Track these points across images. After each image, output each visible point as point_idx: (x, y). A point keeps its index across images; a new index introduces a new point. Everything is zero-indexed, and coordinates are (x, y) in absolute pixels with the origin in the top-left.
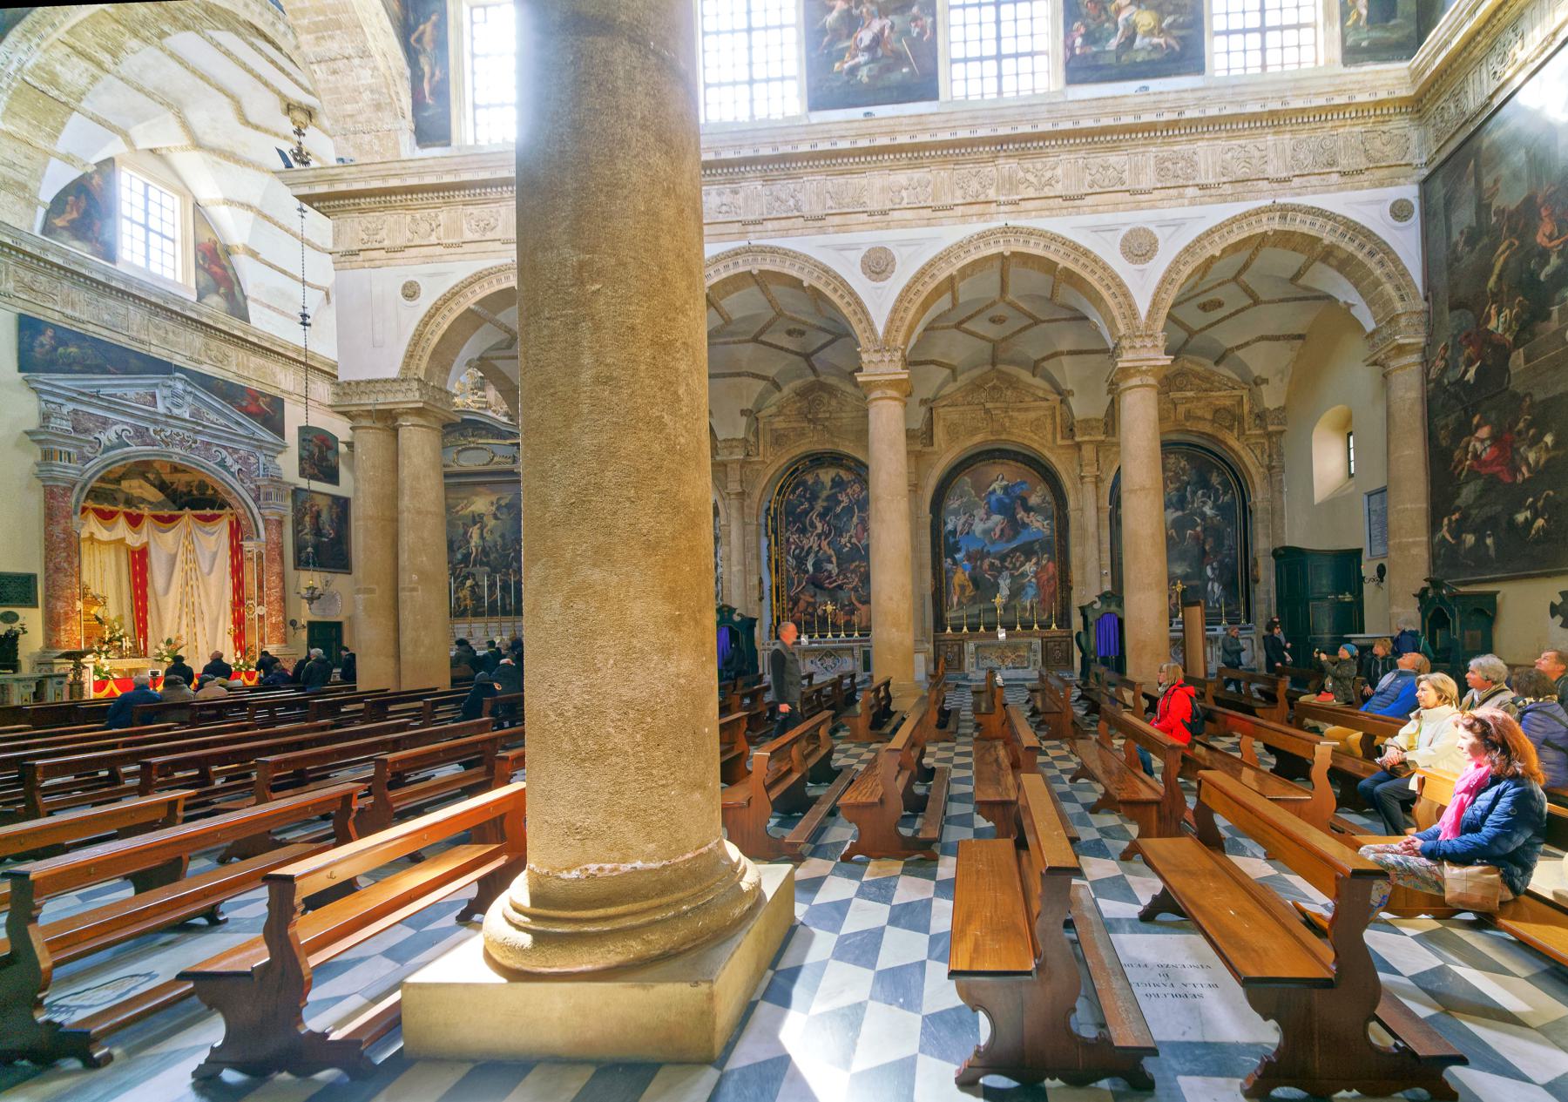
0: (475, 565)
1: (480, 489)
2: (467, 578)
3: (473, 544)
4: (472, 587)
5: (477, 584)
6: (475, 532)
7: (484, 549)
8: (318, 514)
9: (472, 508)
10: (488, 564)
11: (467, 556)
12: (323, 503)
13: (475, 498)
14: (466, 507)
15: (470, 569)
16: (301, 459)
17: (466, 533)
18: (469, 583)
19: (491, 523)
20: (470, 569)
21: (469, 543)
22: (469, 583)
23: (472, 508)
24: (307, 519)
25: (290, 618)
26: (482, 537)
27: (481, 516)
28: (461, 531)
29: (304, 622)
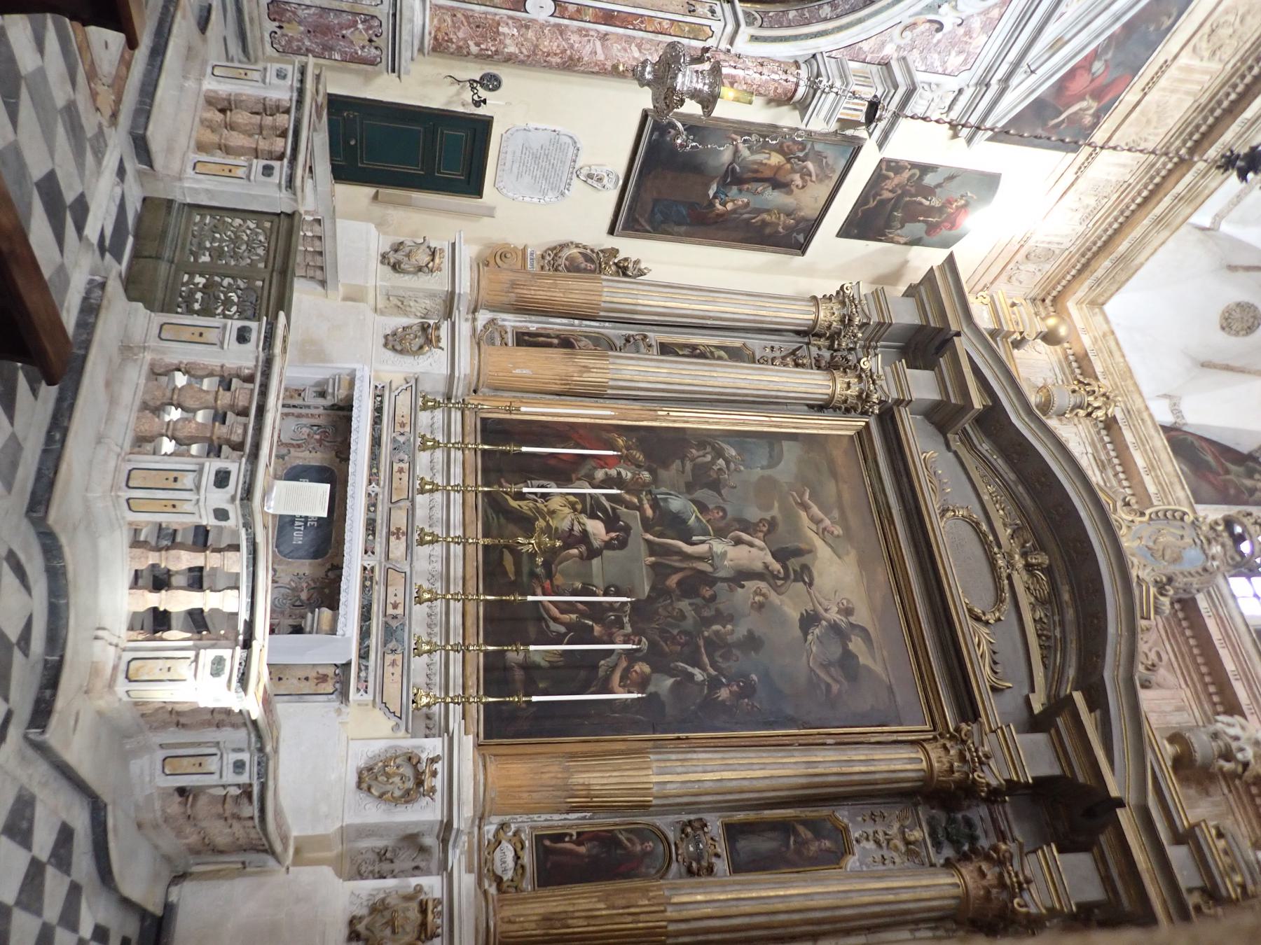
0: (653, 549)
1: (882, 574)
2: (611, 522)
3: (718, 546)
4: (585, 537)
5: (593, 553)
6: (755, 554)
7: (710, 580)
8: (778, 184)
9: (823, 551)
10: (659, 591)
11: (677, 525)
12: (807, 198)
13: (852, 557)
14: (823, 533)
15: (639, 536)
16: (925, 169)
17: (747, 527)
18: (596, 528)
19: (790, 605)
20: (639, 536)
21: (720, 534)
22: (596, 528)
23: (823, 551)
24: (776, 159)
25: (505, 74)
26: (742, 576)
27: (804, 575)
28: (753, 514)
29: (495, 105)
